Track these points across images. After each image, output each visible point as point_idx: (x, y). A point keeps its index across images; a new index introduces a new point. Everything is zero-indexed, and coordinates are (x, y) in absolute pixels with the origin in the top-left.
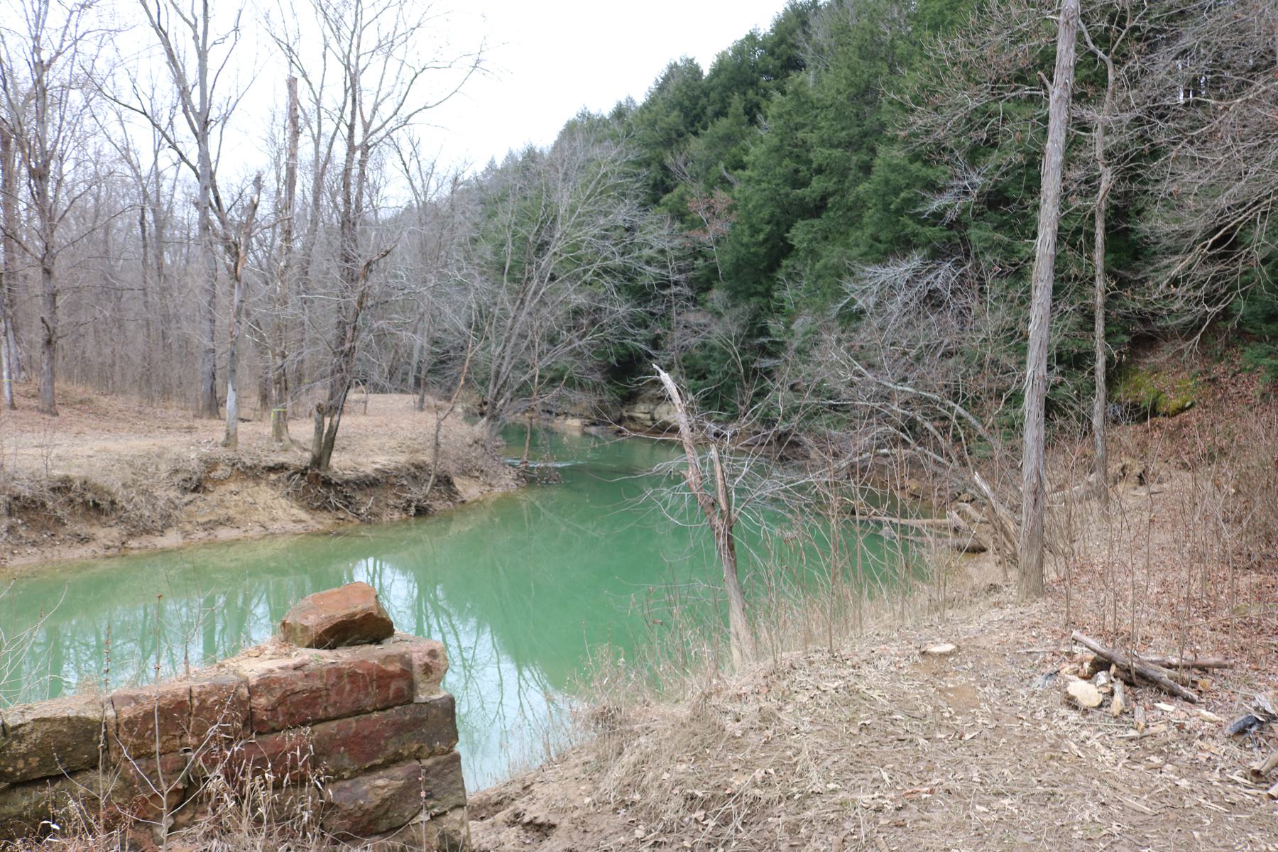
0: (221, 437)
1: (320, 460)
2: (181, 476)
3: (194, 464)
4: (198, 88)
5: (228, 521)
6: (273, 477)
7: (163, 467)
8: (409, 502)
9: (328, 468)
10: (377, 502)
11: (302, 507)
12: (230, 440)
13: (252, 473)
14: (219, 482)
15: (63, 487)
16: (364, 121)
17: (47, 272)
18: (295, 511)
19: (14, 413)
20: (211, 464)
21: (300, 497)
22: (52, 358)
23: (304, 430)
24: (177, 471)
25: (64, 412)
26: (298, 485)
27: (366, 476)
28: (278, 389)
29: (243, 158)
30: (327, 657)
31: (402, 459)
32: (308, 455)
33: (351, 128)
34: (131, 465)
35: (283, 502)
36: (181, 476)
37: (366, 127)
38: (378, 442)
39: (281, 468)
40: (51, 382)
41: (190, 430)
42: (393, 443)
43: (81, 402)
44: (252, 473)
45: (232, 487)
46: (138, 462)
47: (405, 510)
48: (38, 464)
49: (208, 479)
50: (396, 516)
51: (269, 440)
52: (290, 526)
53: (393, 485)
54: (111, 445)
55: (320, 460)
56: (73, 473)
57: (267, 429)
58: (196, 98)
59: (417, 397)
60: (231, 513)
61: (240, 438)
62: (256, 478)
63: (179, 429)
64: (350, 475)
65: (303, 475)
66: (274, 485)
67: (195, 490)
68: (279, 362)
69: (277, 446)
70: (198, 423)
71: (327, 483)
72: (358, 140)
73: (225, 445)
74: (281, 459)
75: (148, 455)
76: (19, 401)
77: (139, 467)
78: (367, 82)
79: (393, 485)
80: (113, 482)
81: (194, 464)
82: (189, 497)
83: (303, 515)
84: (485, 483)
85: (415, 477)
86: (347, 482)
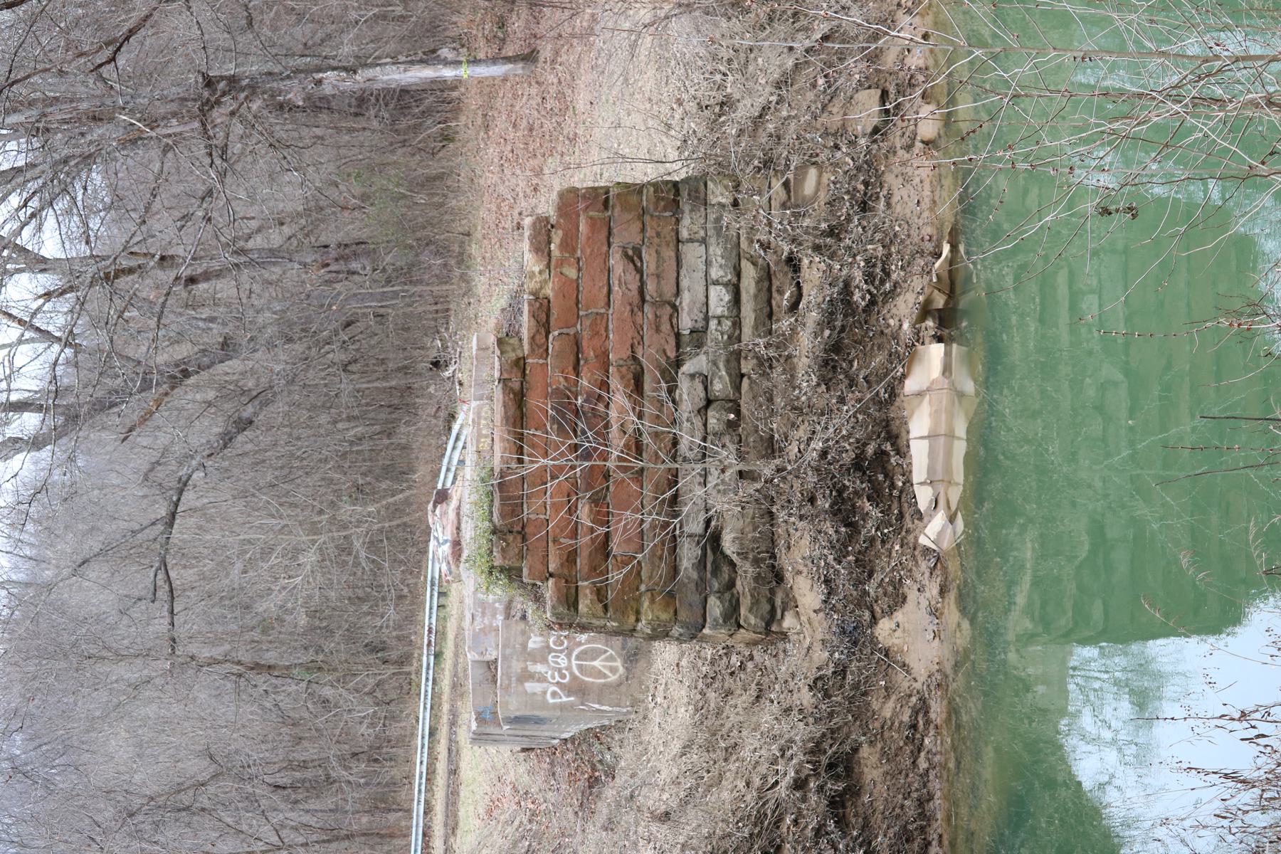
19: (546, 52)
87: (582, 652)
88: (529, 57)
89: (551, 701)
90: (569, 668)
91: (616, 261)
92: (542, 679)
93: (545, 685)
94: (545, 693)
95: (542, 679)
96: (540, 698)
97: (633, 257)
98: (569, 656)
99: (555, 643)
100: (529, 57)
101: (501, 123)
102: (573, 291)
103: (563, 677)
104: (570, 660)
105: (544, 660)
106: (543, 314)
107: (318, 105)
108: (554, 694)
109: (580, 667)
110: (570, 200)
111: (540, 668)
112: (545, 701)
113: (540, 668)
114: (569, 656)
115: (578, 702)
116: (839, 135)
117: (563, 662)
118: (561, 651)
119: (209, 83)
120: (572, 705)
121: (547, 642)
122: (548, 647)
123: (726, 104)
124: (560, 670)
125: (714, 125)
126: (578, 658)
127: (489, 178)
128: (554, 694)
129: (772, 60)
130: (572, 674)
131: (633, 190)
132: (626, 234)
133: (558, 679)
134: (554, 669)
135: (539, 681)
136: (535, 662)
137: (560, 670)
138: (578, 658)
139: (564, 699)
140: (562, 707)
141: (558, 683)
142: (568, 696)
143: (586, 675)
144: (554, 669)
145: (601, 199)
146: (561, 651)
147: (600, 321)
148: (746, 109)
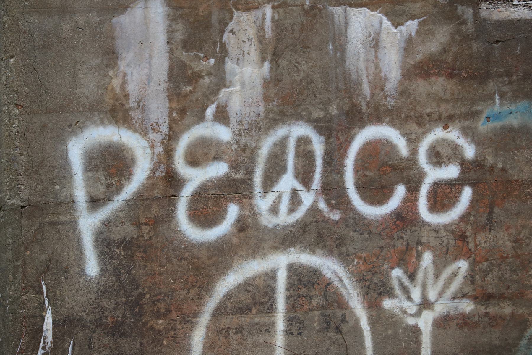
87: (335, 301)
89: (76, 150)
90: (250, 237)
92: (190, 91)
93: (158, 110)
94: (118, 112)
95: (190, 91)
96: (88, 86)
98: (311, 232)
99: (374, 152)
103: (205, 211)
104: (288, 238)
105: (284, 100)
108: (111, 164)
109: (256, 297)
111: (246, 76)
112: (74, 114)
113: (246, 76)
114: (311, 232)
115: (77, 301)
117: (281, 202)
118: (333, 191)
120: (60, 267)
121: (377, 116)
122: (355, 118)
124: (235, 187)
126: (304, 281)
128: (111, 164)
130: (222, 255)
133: (195, 178)
134: (242, 158)
135: (180, 77)
136: (275, 51)
137: (235, 187)
138: (304, 281)
139: (88, 223)
140: (48, 212)
141: (173, 181)
142: (104, 242)
143: (218, 335)
144: (242, 158)
146: (333, 191)
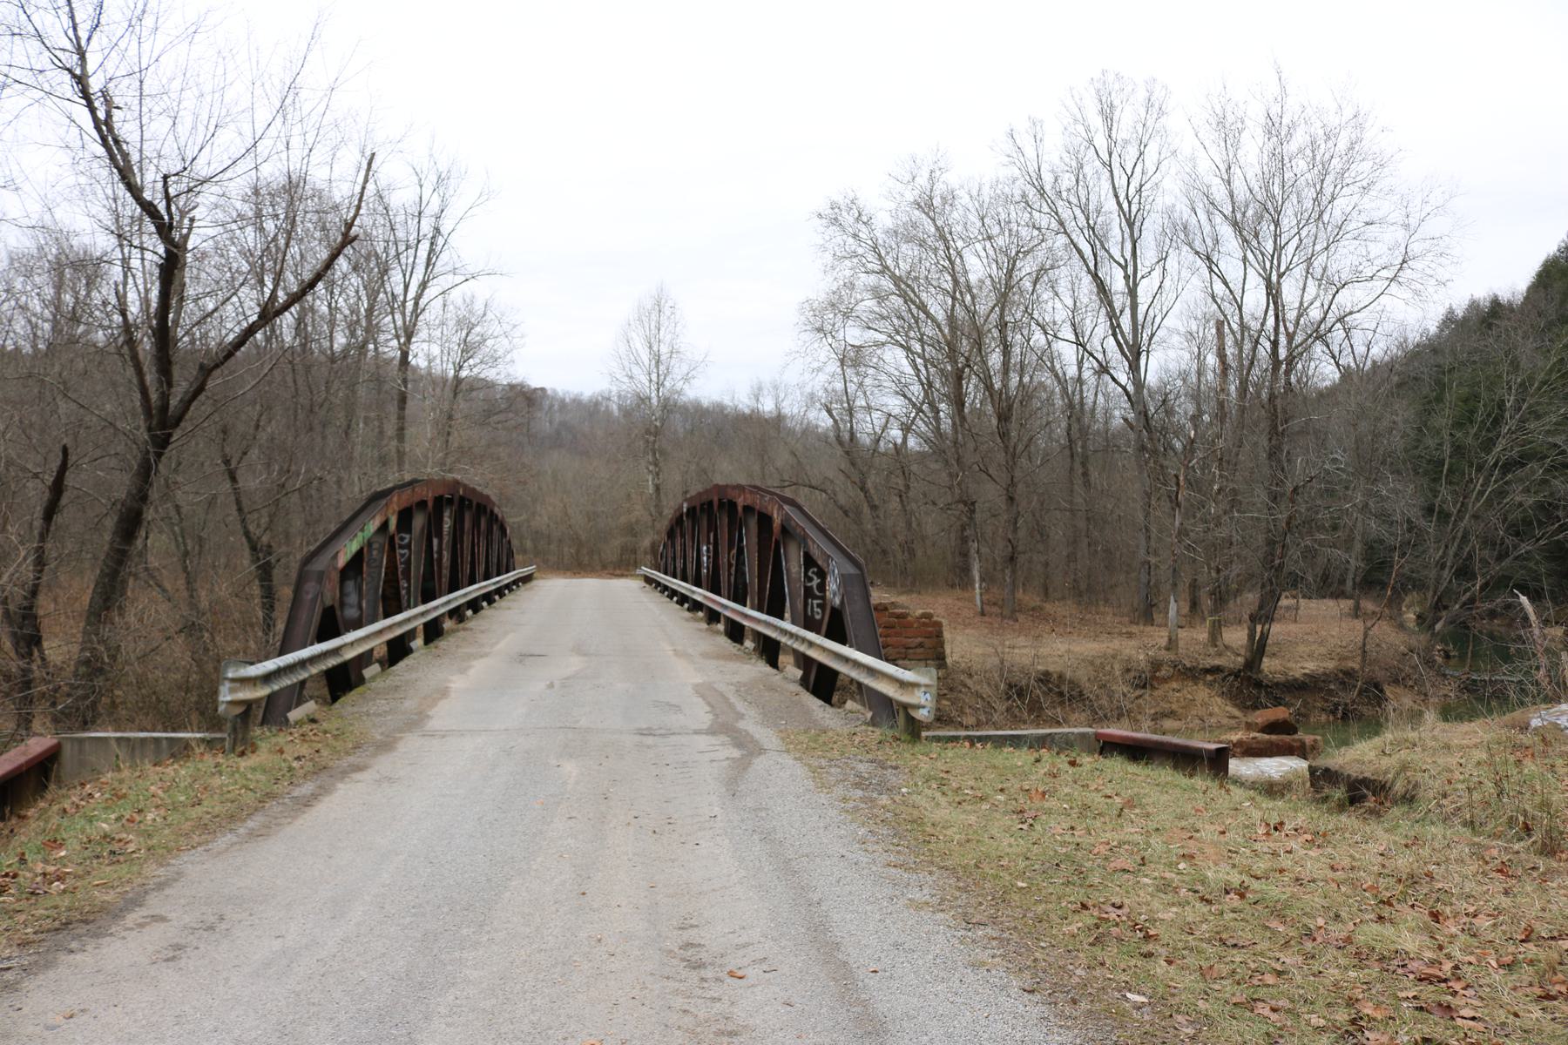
0: (1164, 642)
1: (1253, 662)
2: (1132, 674)
3: (1143, 664)
4: (1128, 311)
5: (1171, 714)
6: (1209, 678)
7: (1117, 666)
8: (1336, 705)
9: (1260, 671)
10: (1305, 703)
11: (1236, 705)
12: (1172, 644)
13: (1192, 674)
14: (1165, 680)
15: (1045, 678)
16: (1288, 334)
17: (1011, 499)
18: (1229, 708)
19: (986, 619)
20: (1156, 665)
21: (1235, 697)
22: (1014, 572)
23: (1236, 637)
24: (1128, 670)
25: (1021, 617)
26: (1232, 686)
27: (1296, 680)
28: (1209, 601)
29: (1166, 361)
30: (1267, 737)
31: (1331, 665)
32: (1240, 660)
33: (1275, 344)
34: (1092, 663)
35: (1219, 700)
36: (1132, 674)
37: (1290, 337)
38: (1307, 650)
39: (1216, 670)
40: (1013, 592)
41: (1130, 635)
42: (1323, 650)
43: (1033, 609)
44: (1192, 674)
45: (1175, 685)
46: (1098, 662)
47: (1333, 712)
48: (1026, 661)
49: (1153, 678)
50: (1324, 717)
51: (1205, 645)
52: (1225, 721)
53: (1321, 689)
54: (1077, 648)
55: (1253, 662)
56: (1051, 669)
57: (1202, 635)
58: (1126, 322)
59: (1350, 603)
60: (1174, 707)
61: (1181, 644)
62: (1195, 679)
63: (1120, 634)
64: (1279, 678)
65: (1237, 676)
66: (1210, 685)
67: (1144, 687)
68: (1214, 574)
69: (1212, 650)
70: (1134, 629)
71: (1259, 685)
72: (1283, 353)
73: (1167, 649)
74: (1217, 662)
75: (1104, 656)
76: (987, 608)
77: (1098, 665)
78: (1290, 292)
79: (1321, 689)
80: (1083, 675)
81: (1143, 664)
82: (1138, 692)
83: (1236, 712)
84: (1419, 693)
85: (1343, 683)
86: (1277, 684)
88: (983, 614)
91: (919, 640)
97: (921, 645)
100: (983, 614)
101: (960, 604)
102: (910, 625)
106: (899, 616)
107: (964, 540)
110: (939, 624)
116: (962, 712)
119: (973, 503)
123: (971, 676)
125: (963, 672)
127: (941, 600)
129: (986, 690)
131: (942, 644)
132: (928, 643)
145: (939, 635)
147: (897, 634)
148: (969, 682)
